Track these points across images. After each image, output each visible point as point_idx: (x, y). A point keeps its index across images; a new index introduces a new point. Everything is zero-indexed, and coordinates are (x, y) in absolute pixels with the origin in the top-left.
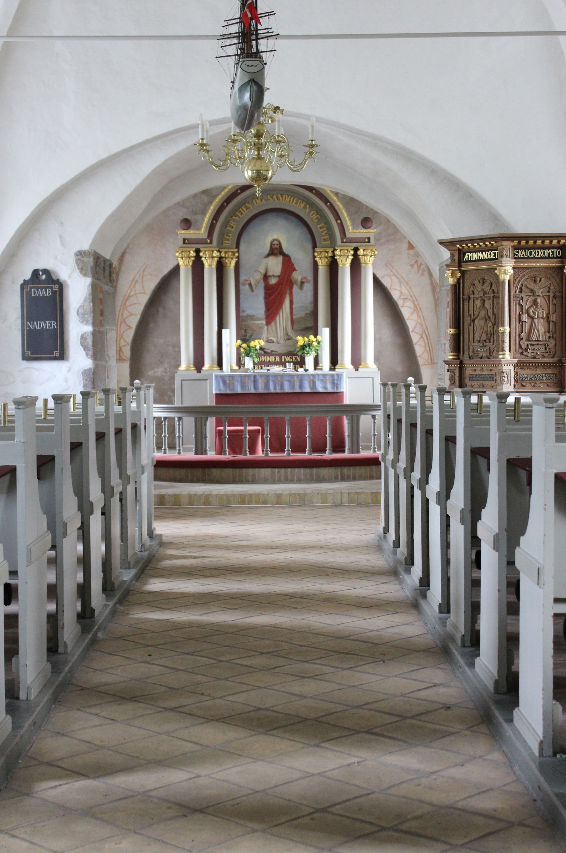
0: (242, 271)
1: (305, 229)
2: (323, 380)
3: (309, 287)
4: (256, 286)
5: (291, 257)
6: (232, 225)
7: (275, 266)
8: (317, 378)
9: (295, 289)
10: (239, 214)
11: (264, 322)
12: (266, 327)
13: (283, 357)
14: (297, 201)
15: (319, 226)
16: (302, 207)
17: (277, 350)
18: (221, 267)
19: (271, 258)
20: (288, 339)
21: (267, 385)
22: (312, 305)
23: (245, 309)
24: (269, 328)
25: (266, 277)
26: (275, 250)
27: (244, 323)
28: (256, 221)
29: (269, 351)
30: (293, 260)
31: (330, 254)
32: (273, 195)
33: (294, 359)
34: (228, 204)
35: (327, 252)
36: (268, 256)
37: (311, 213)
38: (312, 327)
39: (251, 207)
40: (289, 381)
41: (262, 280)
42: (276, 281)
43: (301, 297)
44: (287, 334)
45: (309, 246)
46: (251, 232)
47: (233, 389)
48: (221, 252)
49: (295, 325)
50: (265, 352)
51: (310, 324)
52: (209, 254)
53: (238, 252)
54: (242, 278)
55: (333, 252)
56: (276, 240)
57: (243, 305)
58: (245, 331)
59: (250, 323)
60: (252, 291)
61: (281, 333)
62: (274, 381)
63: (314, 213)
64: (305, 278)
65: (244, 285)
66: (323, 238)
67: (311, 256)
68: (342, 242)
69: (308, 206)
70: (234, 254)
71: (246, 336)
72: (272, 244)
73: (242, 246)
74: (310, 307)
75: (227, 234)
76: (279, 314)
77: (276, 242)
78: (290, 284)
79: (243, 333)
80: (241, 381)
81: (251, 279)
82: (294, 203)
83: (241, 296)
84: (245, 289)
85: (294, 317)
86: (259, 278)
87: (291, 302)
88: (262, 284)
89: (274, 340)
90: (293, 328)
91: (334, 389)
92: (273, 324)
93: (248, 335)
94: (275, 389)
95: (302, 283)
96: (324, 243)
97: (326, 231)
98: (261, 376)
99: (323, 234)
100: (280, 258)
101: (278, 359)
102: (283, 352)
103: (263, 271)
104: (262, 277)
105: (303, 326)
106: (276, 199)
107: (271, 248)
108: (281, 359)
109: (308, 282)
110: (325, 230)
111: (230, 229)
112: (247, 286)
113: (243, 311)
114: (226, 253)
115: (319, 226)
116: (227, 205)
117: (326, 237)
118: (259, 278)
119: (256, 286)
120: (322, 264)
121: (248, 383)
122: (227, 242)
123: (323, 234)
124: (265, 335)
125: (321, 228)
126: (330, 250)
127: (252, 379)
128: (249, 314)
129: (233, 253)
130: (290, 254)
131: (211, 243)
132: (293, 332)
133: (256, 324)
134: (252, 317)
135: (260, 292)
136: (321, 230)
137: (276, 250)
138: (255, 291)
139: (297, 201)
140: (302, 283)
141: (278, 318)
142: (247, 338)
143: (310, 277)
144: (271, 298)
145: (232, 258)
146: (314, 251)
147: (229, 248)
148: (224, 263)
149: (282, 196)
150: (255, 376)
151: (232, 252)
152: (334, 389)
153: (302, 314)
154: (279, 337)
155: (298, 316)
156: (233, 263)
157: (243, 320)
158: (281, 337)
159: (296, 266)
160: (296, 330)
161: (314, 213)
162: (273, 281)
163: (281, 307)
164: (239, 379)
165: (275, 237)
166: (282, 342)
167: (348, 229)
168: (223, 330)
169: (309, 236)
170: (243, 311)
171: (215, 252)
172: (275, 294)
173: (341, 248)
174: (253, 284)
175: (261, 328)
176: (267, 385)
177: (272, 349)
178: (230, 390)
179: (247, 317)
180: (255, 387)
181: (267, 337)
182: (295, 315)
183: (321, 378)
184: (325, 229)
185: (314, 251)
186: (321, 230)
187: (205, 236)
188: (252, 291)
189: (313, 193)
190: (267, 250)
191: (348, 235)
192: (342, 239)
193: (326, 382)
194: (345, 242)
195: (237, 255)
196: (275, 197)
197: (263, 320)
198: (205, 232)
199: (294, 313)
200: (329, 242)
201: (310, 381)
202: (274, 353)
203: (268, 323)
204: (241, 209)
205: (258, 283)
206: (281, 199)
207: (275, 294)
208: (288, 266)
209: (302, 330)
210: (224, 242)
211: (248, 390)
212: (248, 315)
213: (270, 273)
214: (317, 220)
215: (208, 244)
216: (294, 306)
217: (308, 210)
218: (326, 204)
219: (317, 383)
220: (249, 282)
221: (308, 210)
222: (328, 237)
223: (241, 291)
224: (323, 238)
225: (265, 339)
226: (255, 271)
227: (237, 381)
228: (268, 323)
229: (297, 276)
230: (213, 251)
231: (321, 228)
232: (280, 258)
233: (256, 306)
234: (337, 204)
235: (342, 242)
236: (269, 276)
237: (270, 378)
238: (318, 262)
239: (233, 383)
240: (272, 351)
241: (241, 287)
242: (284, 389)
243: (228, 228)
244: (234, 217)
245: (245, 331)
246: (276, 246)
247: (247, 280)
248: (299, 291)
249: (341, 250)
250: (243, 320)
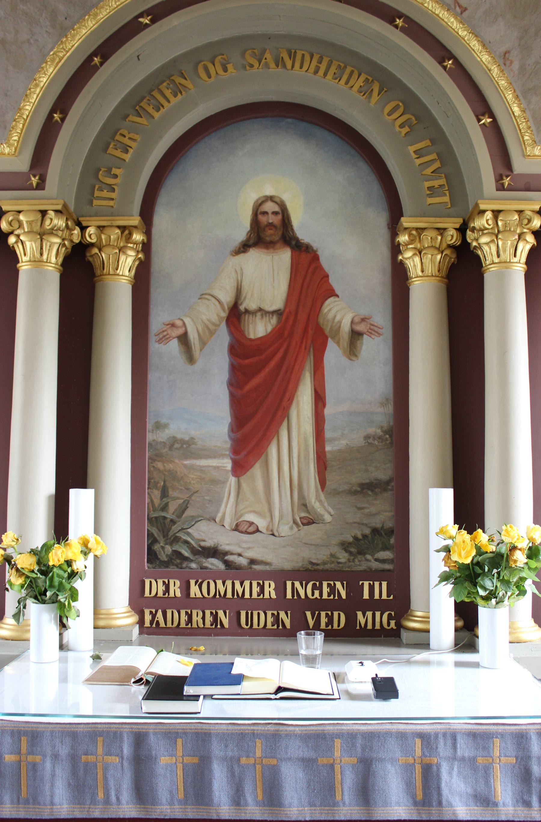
0: (158, 296)
1: (364, 168)
2: (473, 760)
3: (377, 350)
4: (203, 343)
5: (319, 253)
6: (126, 141)
7: (267, 279)
8: (443, 749)
9: (333, 354)
10: (150, 109)
11: (228, 464)
12: (233, 480)
13: (289, 584)
14: (342, 69)
15: (411, 149)
16: (356, 88)
17: (268, 557)
18: (80, 276)
19: (255, 258)
20: (309, 522)
21: (198, 784)
22: (390, 409)
23: (163, 421)
24: (244, 485)
25: (235, 315)
26: (269, 232)
27: (159, 465)
28: (212, 142)
29: (243, 561)
30: (324, 261)
31: (452, 237)
32: (263, 52)
33: (326, 590)
34: (105, 58)
35: (441, 231)
36: (245, 247)
37: (388, 108)
38: (388, 483)
39: (190, 86)
40: (308, 763)
41: (224, 324)
42: (269, 329)
43: (353, 382)
44: (304, 506)
45: (379, 219)
46: (196, 175)
47: (34, 798)
48: (83, 229)
49: (330, 477)
50: (228, 564)
51: (382, 471)
52: (30, 223)
53: (148, 233)
54: (157, 320)
55: (462, 230)
56: (271, 198)
57: (158, 404)
58: (164, 493)
59: (181, 465)
60: (191, 359)
61: (282, 502)
62: (232, 763)
63: (396, 108)
64: (363, 320)
65: (164, 339)
66: (427, 184)
67: (385, 251)
68: (501, 188)
69: (376, 88)
70: (130, 234)
71: (165, 508)
72: (257, 212)
73: (162, 219)
74: (383, 416)
75: (109, 170)
76: (277, 432)
77: (270, 207)
78: (317, 339)
79: (157, 501)
80: (74, 758)
81: (187, 321)
82: (330, 76)
83: (153, 377)
84: (165, 353)
85: (328, 448)
86: (214, 318)
87: (319, 399)
88: (223, 338)
89: (261, 523)
90: (323, 482)
91: (528, 804)
92: (257, 471)
93: (173, 507)
94: (237, 799)
95: (356, 335)
96: (430, 201)
97: (437, 165)
98: (171, 735)
99: (428, 171)
100: (284, 257)
101: (270, 590)
102: (287, 566)
103: (227, 297)
104: (224, 315)
105: (358, 478)
106: (273, 65)
107: (255, 222)
108: (281, 589)
109: (374, 331)
110: (433, 161)
111: (118, 153)
112: (174, 344)
113: (158, 426)
114: (101, 228)
115: (411, 149)
116: (102, 64)
117: (436, 183)
118: (214, 318)
119: (203, 343)
120: (424, 269)
121: (105, 768)
122: (105, 194)
123: (428, 171)
124: (227, 510)
125: (419, 153)
126: (451, 225)
127: (127, 750)
128: (179, 436)
129: (126, 231)
130: (315, 245)
131: (41, 186)
132: (322, 496)
133: (201, 469)
134: (186, 447)
135: (217, 363)
136: (418, 162)
137: (270, 230)
138: (200, 364)
139: (342, 69)
140: (356, 335)
141: (273, 450)
142: (169, 515)
143: (382, 318)
144: (247, 388)
145: (121, 250)
146: (394, 227)
147: (112, 213)
148: (97, 264)
149: (292, 55)
150: (140, 738)
151: (123, 228)
152: (528, 804)
153: (355, 438)
154: (277, 514)
155: (343, 443)
156: (128, 262)
157: (157, 457)
158: (281, 517)
159: (333, 281)
160: (336, 493)
161: (396, 108)
162: (259, 329)
163: (286, 415)
164: (64, 751)
165: (269, 191)
166: (285, 530)
167: (522, 143)
168: (73, 492)
169: (376, 188)
170: (158, 426)
171: (51, 214)
172: (265, 372)
173: (496, 207)
174: (193, 336)
175: (214, 482)
176: (198, 784)
177: (251, 554)
178: (17, 801)
179: (171, 447)
180: (142, 791)
181: (237, 514)
182: (333, 440)
183: (464, 749)
184: (434, 156)
185: (394, 227)
186: (418, 162)
187: (23, 164)
188: (191, 359)
189: (396, 27)
190: (242, 230)
191: (520, 166)
192: (499, 178)
193: (487, 771)
194: (510, 189)
195: (138, 237)
196: (267, 55)
197: (222, 456)
198: (19, 152)
199: (328, 434)
200: (446, 199)
201: (408, 768)
202: (256, 567)
203: (240, 468)
204: (155, 93)
205: (212, 333)
206: (289, 63)
207: (265, 372)
208: (310, 278)
209: (355, 493)
210: (97, 193)
211: (107, 801)
212: (174, 440)
213: (249, 303)
214: (406, 129)
215: (30, 188)
216: (328, 411)
217: (375, 97)
218: (441, 62)
219: (444, 775)
220: (181, 331)
221: (375, 97)
222: (443, 181)
223: (153, 359)
224: (427, 184)
225: (227, 522)
226: (202, 297)
227: (56, 757)
228: (240, 468)
229: (338, 313)
230: (44, 213)
231: (419, 153)
232: (284, 257)
233: (201, 407)
234: (479, 64)
235: (501, 188)
236: (247, 311)
237: (217, 749)
238: (409, 264)
239: (34, 767)
240: (253, 562)
241: (154, 347)
242: (280, 805)
243: (111, 150)
244: (131, 118)
245: (164, 493)
246: (272, 219)
247: (173, 325)
248: (345, 360)
249: (496, 213)
250: (157, 457)
